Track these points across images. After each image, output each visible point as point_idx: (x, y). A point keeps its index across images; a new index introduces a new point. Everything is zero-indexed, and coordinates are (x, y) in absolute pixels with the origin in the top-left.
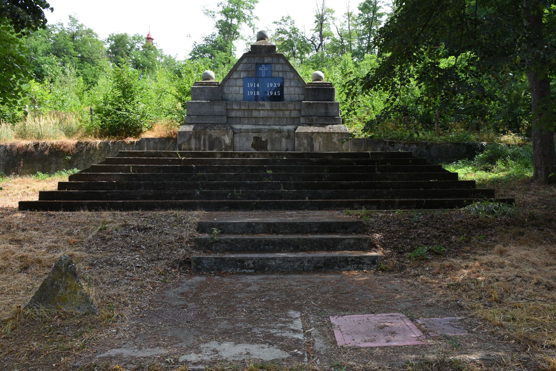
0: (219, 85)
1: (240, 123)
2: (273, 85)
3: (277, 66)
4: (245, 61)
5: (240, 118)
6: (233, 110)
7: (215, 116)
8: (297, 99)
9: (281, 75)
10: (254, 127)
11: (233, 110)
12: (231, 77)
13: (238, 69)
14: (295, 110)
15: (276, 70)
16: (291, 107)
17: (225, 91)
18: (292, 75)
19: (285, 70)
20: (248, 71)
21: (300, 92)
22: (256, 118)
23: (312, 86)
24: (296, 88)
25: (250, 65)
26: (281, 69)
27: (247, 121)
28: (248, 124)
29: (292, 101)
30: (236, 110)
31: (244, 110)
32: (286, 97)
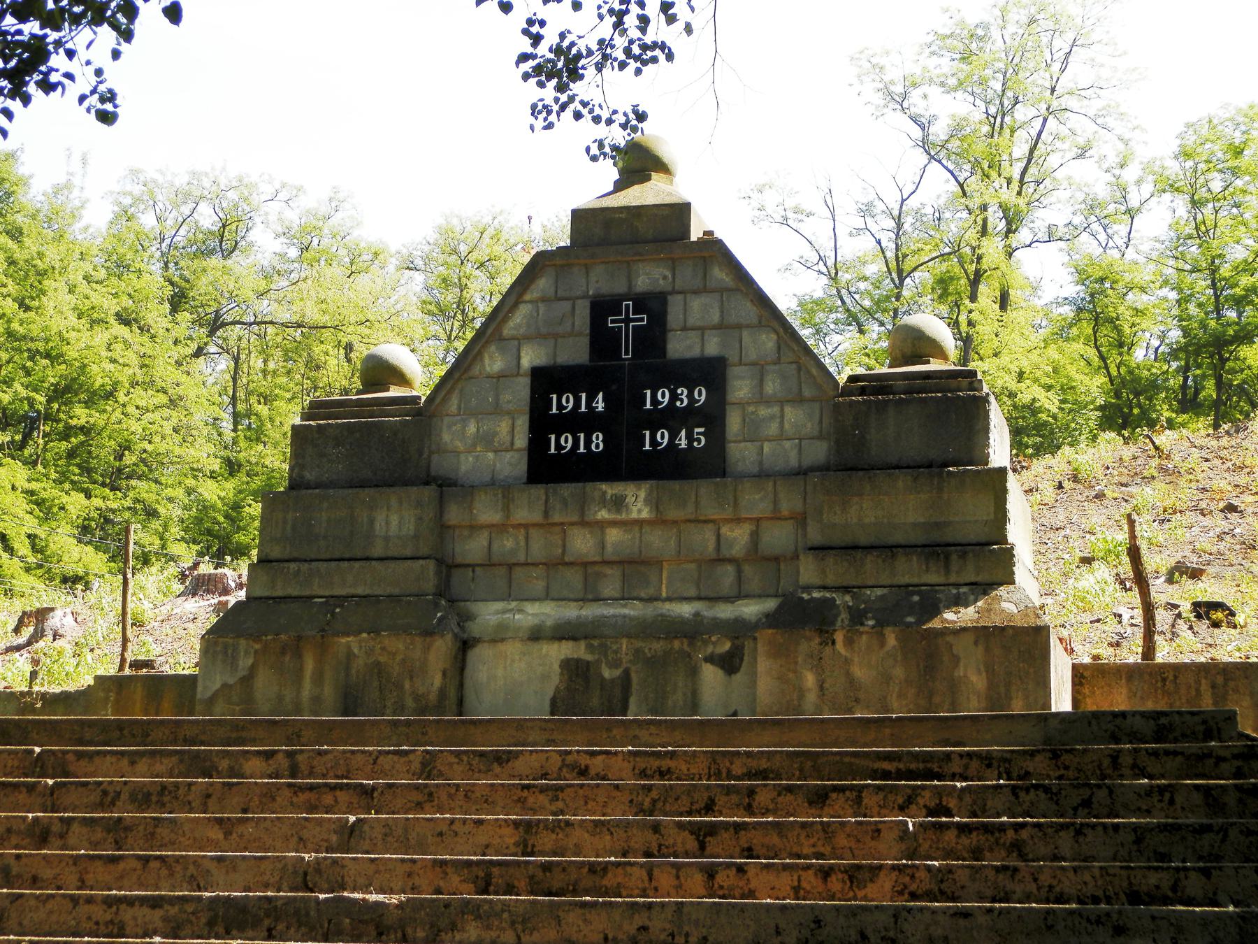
0: (419, 413)
1: (509, 595)
2: (674, 397)
3: (696, 303)
4: (543, 285)
5: (511, 567)
6: (474, 528)
7: (271, 561)
8: (793, 462)
9: (713, 347)
10: (571, 612)
11: (474, 528)
12: (476, 370)
13: (506, 332)
14: (776, 517)
15: (691, 321)
16: (755, 501)
17: (446, 437)
18: (768, 341)
19: (732, 319)
20: (556, 336)
21: (810, 428)
22: (585, 565)
23: (863, 391)
24: (788, 410)
25: (566, 306)
26: (716, 318)
27: (540, 585)
28: (547, 596)
29: (763, 475)
30: (491, 526)
31: (526, 526)
32: (741, 453)
